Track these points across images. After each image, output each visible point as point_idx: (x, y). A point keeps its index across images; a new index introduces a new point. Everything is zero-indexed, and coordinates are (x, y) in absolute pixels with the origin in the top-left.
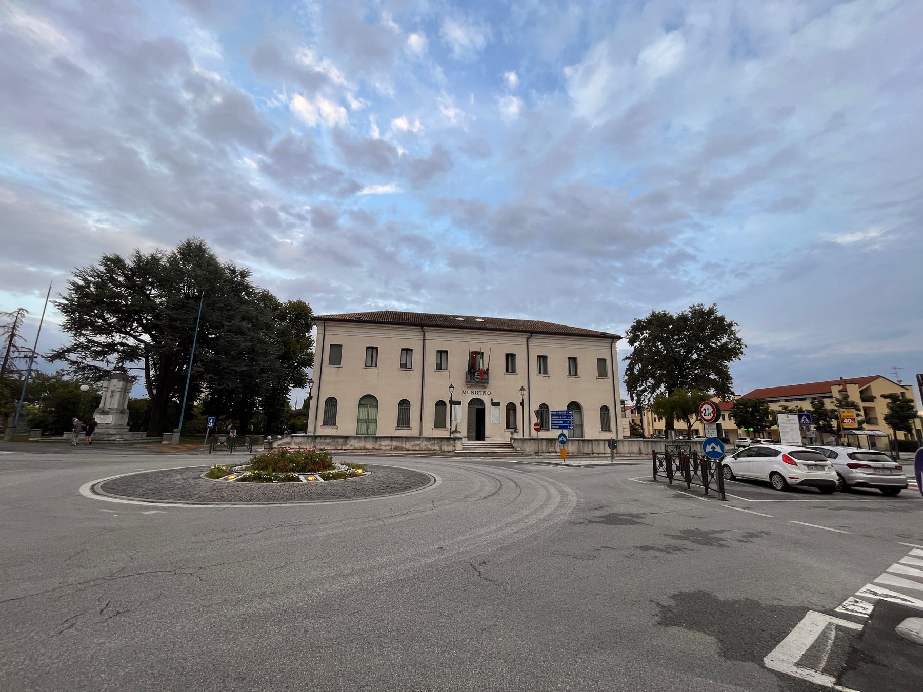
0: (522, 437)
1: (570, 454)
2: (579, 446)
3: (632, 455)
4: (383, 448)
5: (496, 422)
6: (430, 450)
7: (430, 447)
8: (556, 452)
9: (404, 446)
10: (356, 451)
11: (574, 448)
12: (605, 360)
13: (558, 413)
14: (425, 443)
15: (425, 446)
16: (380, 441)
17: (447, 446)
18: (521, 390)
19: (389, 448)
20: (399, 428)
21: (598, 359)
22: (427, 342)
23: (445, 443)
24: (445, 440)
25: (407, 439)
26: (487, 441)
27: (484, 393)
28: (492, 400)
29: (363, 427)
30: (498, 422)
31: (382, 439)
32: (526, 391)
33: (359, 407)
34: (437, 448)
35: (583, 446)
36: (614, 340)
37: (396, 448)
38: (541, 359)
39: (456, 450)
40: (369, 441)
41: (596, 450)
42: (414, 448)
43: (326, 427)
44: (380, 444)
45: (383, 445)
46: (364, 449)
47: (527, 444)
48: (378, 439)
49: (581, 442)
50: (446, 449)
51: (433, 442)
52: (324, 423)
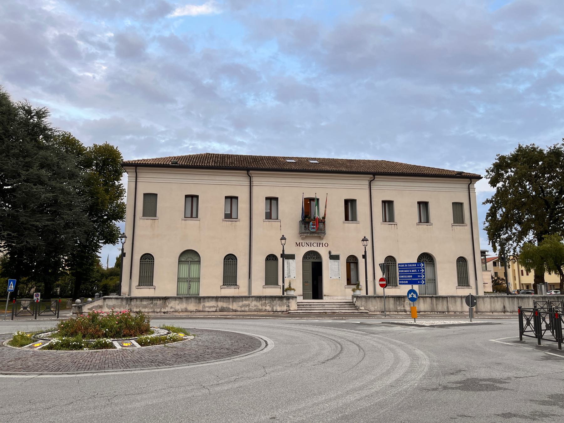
0: (365, 294)
1: (421, 313)
2: (432, 303)
3: (495, 314)
4: (207, 309)
5: (334, 278)
6: (260, 311)
7: (260, 307)
8: (405, 311)
9: (231, 307)
10: (177, 314)
11: (426, 305)
12: (461, 204)
13: (406, 266)
14: (254, 303)
15: (255, 306)
16: (204, 302)
17: (280, 306)
18: (363, 240)
19: (214, 309)
20: (225, 287)
21: (453, 203)
22: (255, 189)
23: (278, 302)
24: (277, 299)
25: (235, 298)
26: (325, 299)
27: (321, 245)
28: (330, 253)
29: (184, 286)
30: (337, 277)
31: (206, 300)
32: (369, 243)
33: (179, 264)
34: (268, 308)
35: (436, 304)
36: (472, 180)
37: (222, 310)
38: (387, 204)
39: (290, 310)
40: (191, 303)
41: (452, 308)
42: (243, 309)
43: (141, 287)
44: (204, 305)
45: (207, 307)
46: (186, 311)
47: (372, 302)
48: (202, 300)
49: (434, 299)
50: (279, 309)
51: (264, 301)
52: (139, 283)
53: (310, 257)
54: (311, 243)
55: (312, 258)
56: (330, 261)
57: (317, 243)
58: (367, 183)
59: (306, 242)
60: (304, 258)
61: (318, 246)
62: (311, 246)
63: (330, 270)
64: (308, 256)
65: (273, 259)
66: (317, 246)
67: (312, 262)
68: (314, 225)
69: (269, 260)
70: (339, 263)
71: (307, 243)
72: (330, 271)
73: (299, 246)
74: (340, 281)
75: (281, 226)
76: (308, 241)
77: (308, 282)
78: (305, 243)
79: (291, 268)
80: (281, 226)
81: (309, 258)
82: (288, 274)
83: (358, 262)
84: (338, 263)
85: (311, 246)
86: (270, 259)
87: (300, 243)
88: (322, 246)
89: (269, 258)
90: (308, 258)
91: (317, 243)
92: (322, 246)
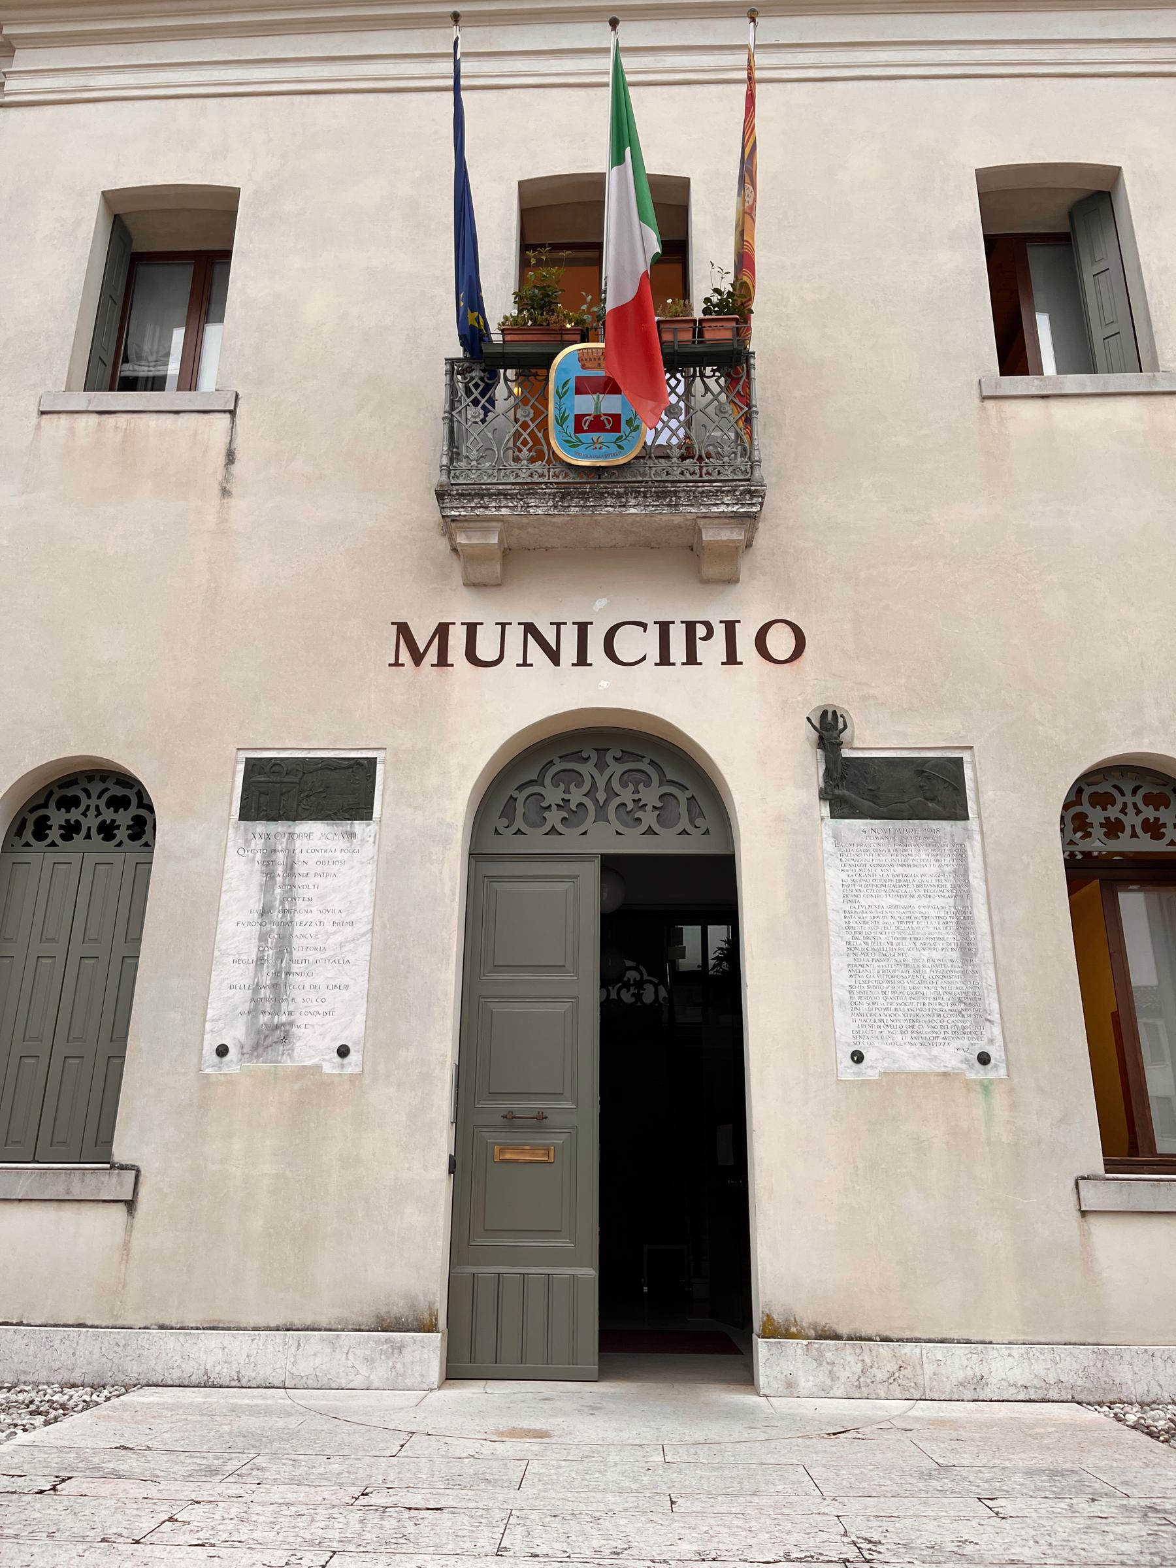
27: (712, 651)
54: (583, 628)
55: (601, 815)
56: (837, 837)
57: (664, 627)
60: (508, 812)
61: (678, 651)
62: (582, 660)
63: (837, 944)
65: (107, 831)
66: (665, 660)
67: (602, 855)
69: (54, 834)
70: (961, 854)
71: (530, 629)
72: (838, 963)
73: (432, 656)
74: (999, 1100)
77: (541, 1117)
78: (515, 635)
81: (573, 815)
82: (253, 1013)
84: (948, 862)
85: (582, 660)
86: (70, 830)
87: (442, 631)
88: (731, 658)
89: (58, 818)
90: (554, 817)
91: (664, 627)
92: (731, 658)
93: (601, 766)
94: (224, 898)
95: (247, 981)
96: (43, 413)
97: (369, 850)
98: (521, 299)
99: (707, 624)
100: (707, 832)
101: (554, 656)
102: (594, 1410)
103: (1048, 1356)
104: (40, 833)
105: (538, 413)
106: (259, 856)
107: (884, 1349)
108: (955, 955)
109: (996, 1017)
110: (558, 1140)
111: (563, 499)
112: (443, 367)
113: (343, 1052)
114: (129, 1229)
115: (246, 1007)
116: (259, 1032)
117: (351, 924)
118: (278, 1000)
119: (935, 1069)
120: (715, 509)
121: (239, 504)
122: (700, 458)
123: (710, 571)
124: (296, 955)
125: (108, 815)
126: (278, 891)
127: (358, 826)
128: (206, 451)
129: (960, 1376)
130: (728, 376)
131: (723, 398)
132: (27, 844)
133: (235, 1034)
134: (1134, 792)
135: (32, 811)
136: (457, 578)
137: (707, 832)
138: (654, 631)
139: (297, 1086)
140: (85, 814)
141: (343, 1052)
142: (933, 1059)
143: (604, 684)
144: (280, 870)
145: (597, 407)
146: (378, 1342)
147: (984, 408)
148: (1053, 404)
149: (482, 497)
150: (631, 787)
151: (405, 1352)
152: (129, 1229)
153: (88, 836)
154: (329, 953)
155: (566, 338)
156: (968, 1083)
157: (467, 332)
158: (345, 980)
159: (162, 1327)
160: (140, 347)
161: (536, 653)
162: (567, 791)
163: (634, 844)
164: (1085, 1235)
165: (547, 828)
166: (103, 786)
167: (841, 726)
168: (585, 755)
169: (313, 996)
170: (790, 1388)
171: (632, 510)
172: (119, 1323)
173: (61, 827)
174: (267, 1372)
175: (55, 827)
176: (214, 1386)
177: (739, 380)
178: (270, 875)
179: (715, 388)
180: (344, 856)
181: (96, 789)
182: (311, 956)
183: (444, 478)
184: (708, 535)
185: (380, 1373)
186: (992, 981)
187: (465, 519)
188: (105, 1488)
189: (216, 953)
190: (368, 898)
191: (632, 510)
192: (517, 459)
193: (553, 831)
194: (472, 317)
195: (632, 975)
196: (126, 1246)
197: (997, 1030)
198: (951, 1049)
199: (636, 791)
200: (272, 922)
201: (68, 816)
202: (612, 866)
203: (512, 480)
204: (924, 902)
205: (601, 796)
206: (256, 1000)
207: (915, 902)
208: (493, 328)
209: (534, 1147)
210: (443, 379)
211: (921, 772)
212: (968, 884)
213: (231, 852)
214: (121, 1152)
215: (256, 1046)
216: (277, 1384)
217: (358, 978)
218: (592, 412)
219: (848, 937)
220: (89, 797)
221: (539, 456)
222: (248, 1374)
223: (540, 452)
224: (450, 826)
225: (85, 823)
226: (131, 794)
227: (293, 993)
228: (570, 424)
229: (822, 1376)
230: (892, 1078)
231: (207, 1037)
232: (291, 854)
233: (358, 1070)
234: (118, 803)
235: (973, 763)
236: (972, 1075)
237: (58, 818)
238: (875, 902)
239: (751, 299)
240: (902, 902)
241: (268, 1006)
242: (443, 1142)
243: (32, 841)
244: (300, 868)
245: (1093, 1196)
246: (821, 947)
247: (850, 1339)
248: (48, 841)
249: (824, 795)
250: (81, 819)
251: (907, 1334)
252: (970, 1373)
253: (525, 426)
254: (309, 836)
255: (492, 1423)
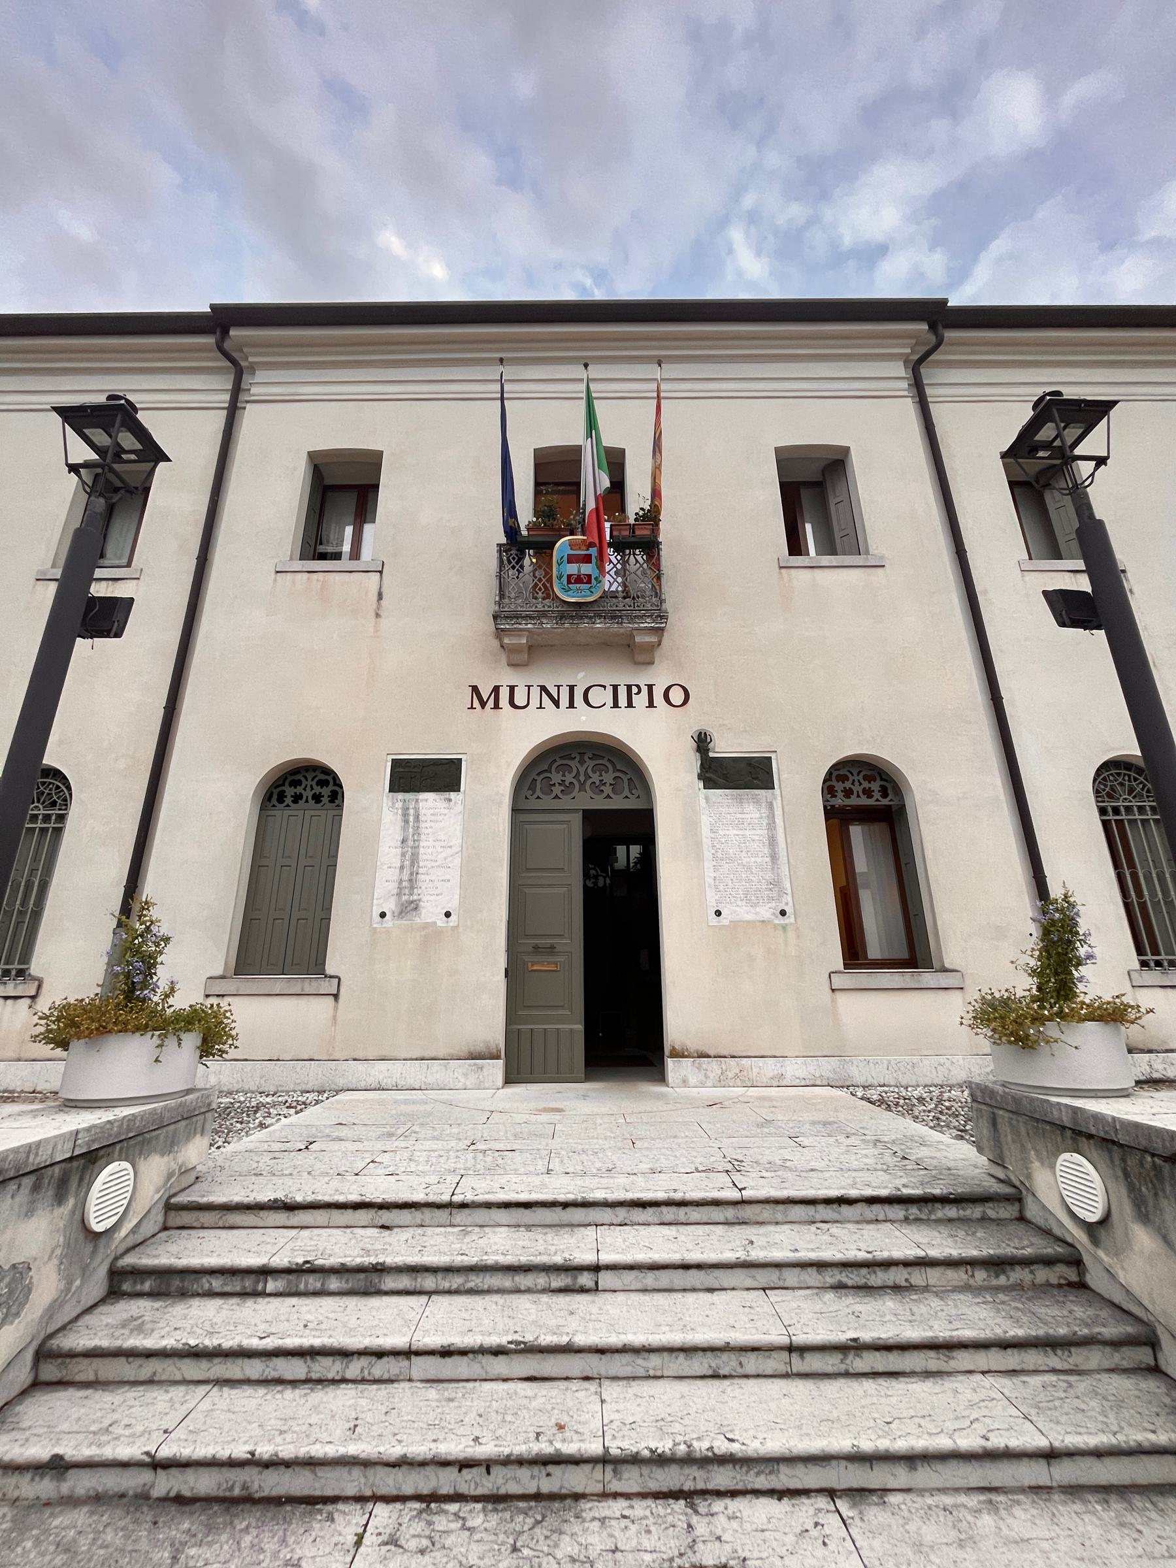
22: (252, 418)
27: (641, 700)
28: (702, 742)
30: (766, 912)
53: (569, 778)
54: (572, 688)
55: (582, 788)
56: (707, 799)
57: (615, 688)
58: (899, 370)
59: (536, 681)
60: (532, 788)
62: (571, 705)
63: (708, 855)
64: (556, 778)
65: (317, 798)
66: (616, 705)
67: (584, 811)
68: (587, 559)
69: (288, 800)
70: (771, 806)
71: (543, 688)
72: (708, 865)
73: (491, 703)
74: (791, 934)
75: (380, 596)
76: (556, 677)
77: (552, 947)
78: (535, 692)
79: (427, 848)
80: (380, 596)
81: (567, 789)
82: (399, 895)
83: (902, 808)
84: (764, 811)
85: (571, 705)
86: (297, 798)
87: (496, 690)
88: (651, 704)
89: (290, 791)
90: (557, 790)
91: (615, 688)
92: (651, 704)
93: (582, 762)
94: (382, 834)
95: (396, 878)
96: (278, 572)
97: (459, 808)
98: (536, 513)
99: (638, 686)
100: (638, 797)
101: (557, 703)
102: (585, 1097)
103: (815, 1063)
104: (281, 798)
105: (546, 573)
106: (400, 811)
107: (732, 1062)
108: (768, 859)
109: (789, 891)
110: (561, 959)
111: (560, 620)
112: (496, 548)
113: (448, 915)
114: (336, 1009)
115: (395, 891)
116: (402, 905)
117: (450, 847)
118: (412, 888)
119: (758, 919)
120: (642, 625)
121: (384, 621)
122: (634, 598)
123: (640, 658)
124: (421, 864)
125: (317, 790)
126: (411, 830)
127: (453, 795)
128: (367, 593)
129: (771, 1074)
130: (647, 554)
131: (645, 565)
132: (274, 806)
133: (390, 906)
134: (859, 773)
135: (276, 788)
136: (504, 659)
137: (638, 797)
138: (610, 690)
139: (423, 933)
140: (305, 789)
141: (448, 915)
142: (756, 914)
143: (583, 718)
144: (411, 819)
145: (579, 570)
146: (470, 1065)
147: (780, 573)
148: (816, 571)
149: (518, 618)
150: (598, 773)
151: (484, 1070)
152: (336, 1009)
153: (307, 801)
154: (438, 863)
155: (562, 533)
156: (775, 927)
157: (508, 530)
158: (448, 877)
159: (355, 1060)
160: (328, 536)
161: (546, 700)
162: (564, 775)
163: (600, 803)
164: (833, 1001)
165: (553, 795)
166: (314, 774)
167: (709, 740)
168: (573, 756)
169: (431, 885)
170: (685, 1083)
171: (598, 626)
172: (332, 1058)
173: (292, 796)
174: (411, 1082)
175: (289, 797)
176: (383, 1090)
177: (653, 557)
178: (406, 822)
179: (641, 561)
180: (446, 811)
181: (310, 776)
182: (429, 864)
183: (497, 608)
184: (638, 639)
185: (471, 1081)
186: (787, 873)
187: (509, 630)
188: (336, 1146)
189: (379, 863)
190: (459, 834)
191: (598, 626)
192: (536, 598)
193: (557, 797)
194: (511, 521)
195: (592, 872)
196: (334, 1018)
197: (789, 898)
198: (766, 908)
199: (601, 775)
200: (408, 847)
201: (295, 790)
202: (589, 816)
203: (533, 609)
204: (753, 832)
205: (582, 779)
206: (400, 888)
207: (747, 833)
208: (523, 527)
209: (549, 963)
210: (496, 555)
211: (750, 765)
212: (774, 823)
213: (385, 809)
214: (330, 969)
215: (401, 912)
216: (417, 1087)
217: (455, 876)
218: (576, 573)
219: (713, 851)
220: (307, 780)
221: (548, 597)
222: (401, 1083)
223: (549, 594)
224: (503, 795)
225: (305, 794)
226: (330, 778)
227: (420, 884)
228: (565, 579)
229: (701, 1077)
230: (735, 924)
231: (374, 908)
232: (417, 810)
233: (456, 924)
234: (323, 783)
235: (777, 759)
236: (777, 922)
237: (290, 791)
238: (727, 832)
239: (660, 514)
240: (740, 832)
241: (407, 891)
242: (502, 962)
243: (276, 804)
244: (422, 818)
245: (838, 981)
246: (699, 858)
247: (715, 1057)
248: (285, 804)
249: (700, 777)
250: (303, 792)
251: (744, 1054)
252: (776, 1072)
253: (540, 580)
254: (426, 800)
255: (533, 1105)
